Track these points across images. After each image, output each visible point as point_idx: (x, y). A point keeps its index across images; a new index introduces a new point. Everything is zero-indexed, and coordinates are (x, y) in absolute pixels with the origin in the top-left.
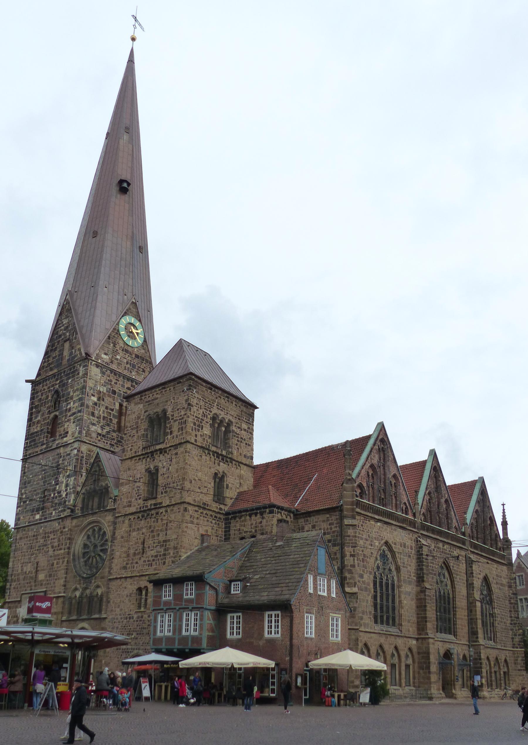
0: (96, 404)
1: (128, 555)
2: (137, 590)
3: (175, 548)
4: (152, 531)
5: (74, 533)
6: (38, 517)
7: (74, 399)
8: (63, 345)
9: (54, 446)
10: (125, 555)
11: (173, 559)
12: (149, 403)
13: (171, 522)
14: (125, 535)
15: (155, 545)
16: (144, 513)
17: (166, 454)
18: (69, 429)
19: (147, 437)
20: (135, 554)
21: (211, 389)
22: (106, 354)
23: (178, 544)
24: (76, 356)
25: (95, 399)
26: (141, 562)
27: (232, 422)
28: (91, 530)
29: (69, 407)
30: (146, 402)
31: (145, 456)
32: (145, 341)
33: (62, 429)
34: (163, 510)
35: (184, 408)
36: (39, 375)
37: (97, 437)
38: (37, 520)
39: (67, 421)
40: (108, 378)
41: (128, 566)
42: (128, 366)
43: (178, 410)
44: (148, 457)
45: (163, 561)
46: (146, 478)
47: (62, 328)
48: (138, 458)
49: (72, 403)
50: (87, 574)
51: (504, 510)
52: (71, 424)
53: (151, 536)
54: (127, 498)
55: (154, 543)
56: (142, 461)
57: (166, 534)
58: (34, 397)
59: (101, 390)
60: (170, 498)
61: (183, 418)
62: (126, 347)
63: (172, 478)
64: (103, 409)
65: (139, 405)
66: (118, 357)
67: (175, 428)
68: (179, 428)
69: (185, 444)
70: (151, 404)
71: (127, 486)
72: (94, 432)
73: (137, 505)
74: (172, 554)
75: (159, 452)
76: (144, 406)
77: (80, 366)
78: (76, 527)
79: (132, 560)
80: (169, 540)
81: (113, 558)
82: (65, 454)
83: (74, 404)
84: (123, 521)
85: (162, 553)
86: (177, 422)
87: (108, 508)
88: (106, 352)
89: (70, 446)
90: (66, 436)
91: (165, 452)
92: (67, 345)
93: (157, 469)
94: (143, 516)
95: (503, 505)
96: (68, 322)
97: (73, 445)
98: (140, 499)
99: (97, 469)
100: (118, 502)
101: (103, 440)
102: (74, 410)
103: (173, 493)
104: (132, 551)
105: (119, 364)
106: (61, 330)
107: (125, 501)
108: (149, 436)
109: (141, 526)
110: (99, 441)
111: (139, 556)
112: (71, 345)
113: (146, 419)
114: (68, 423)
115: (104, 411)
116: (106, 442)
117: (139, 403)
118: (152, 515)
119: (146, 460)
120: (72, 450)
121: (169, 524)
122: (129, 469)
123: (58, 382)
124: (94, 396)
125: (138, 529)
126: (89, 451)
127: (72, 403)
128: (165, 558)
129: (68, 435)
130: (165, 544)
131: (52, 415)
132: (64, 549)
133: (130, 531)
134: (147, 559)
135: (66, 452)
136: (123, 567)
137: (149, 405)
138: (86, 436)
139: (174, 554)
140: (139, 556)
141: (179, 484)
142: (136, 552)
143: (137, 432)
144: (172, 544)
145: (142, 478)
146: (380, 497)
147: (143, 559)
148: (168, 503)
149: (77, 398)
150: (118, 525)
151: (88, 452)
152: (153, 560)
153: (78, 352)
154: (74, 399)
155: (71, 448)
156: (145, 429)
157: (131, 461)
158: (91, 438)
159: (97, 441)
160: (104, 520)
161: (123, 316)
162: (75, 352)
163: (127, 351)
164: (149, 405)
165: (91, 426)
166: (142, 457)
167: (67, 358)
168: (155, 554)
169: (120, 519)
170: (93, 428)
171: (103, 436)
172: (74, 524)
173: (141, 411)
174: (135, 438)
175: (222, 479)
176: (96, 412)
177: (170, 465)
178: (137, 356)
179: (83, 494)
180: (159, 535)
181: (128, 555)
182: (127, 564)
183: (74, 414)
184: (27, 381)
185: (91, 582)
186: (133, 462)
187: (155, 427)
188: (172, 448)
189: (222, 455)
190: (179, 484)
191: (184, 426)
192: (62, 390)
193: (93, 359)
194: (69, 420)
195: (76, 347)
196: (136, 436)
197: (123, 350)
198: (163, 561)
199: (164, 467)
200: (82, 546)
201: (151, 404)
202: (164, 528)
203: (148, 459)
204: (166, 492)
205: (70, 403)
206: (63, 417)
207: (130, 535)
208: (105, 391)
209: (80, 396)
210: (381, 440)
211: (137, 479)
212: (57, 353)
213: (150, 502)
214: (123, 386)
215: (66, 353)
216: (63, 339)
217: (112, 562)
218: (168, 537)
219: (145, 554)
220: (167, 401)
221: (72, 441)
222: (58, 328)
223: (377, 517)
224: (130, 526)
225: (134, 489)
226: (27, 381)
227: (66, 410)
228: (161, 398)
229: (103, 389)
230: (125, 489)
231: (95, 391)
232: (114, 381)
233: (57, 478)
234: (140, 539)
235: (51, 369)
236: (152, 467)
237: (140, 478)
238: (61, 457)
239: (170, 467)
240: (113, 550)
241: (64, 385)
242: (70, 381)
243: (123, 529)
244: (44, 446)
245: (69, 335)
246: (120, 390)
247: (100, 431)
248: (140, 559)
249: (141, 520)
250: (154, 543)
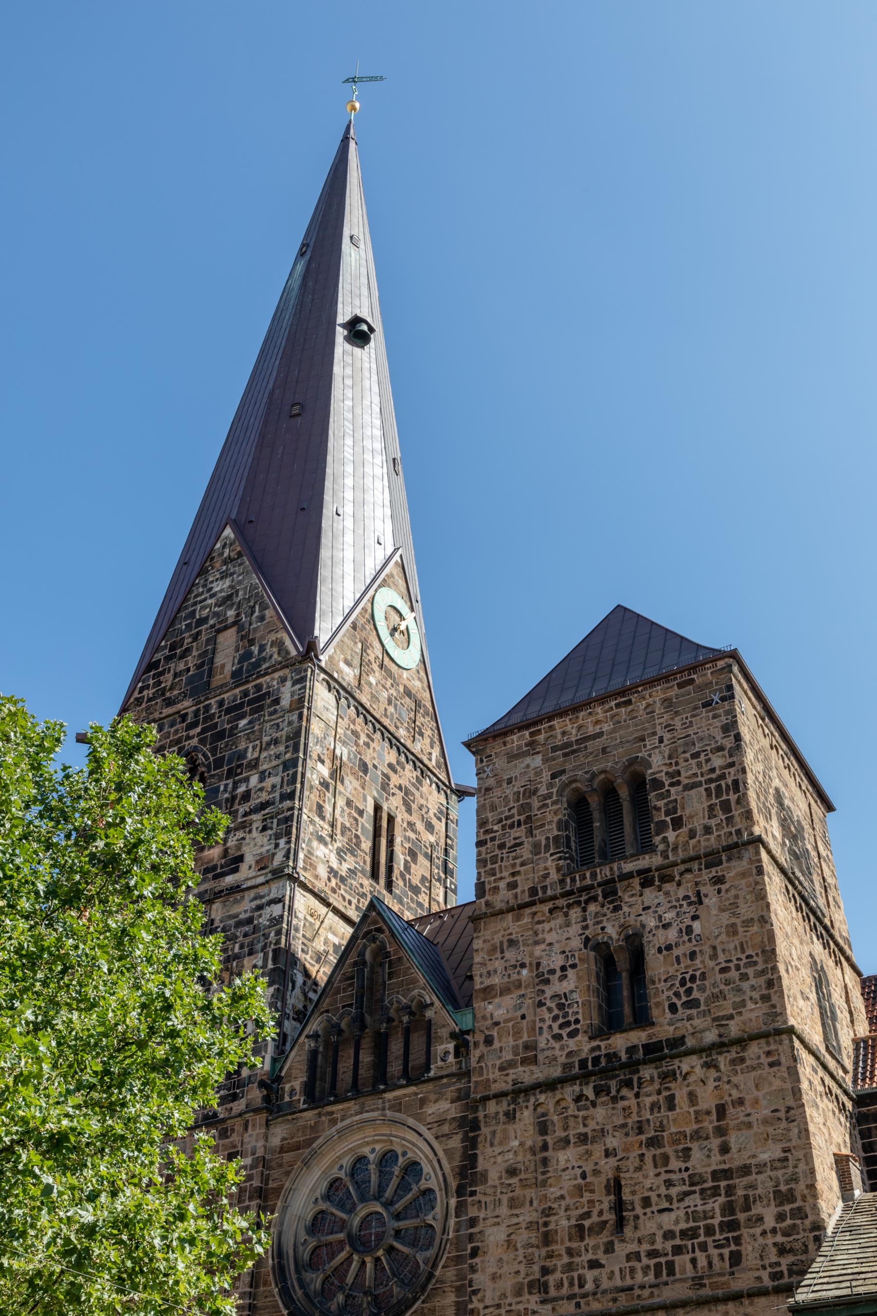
0: (325, 785)
1: (547, 1239)
3: (783, 1197)
4: (654, 1142)
5: (275, 1174)
7: (261, 768)
10: (533, 1237)
11: (779, 1238)
12: (569, 749)
13: (741, 1102)
14: (524, 1159)
15: (674, 1191)
17: (667, 887)
18: (245, 849)
19: (568, 846)
20: (580, 1232)
21: (763, 719)
22: (348, 663)
23: (794, 1179)
25: (324, 771)
26: (615, 1263)
29: (242, 789)
30: (555, 749)
31: (579, 897)
34: (691, 1064)
35: (721, 749)
37: (329, 879)
40: (352, 726)
41: (552, 1279)
43: (696, 755)
44: (594, 899)
45: (726, 1252)
46: (590, 963)
47: (209, 601)
48: (546, 908)
49: (254, 780)
52: (255, 834)
53: (648, 1159)
54: (517, 1034)
55: (669, 1184)
56: (566, 915)
57: (725, 1149)
59: (338, 752)
60: (720, 1021)
61: (722, 777)
63: (714, 956)
64: (341, 802)
65: (528, 760)
66: (373, 680)
67: (696, 805)
68: (711, 808)
69: (751, 848)
70: (573, 752)
71: (509, 1001)
72: (323, 863)
74: (770, 1222)
75: (636, 882)
76: (545, 761)
77: (283, 680)
78: (282, 1150)
79: (570, 1252)
80: (745, 1170)
81: (475, 1253)
82: (232, 922)
83: (262, 780)
84: (511, 1116)
85: (716, 1222)
86: (702, 789)
87: (432, 1074)
88: (349, 658)
89: (252, 893)
90: (236, 870)
96: (231, 587)
97: (262, 890)
98: (572, 1034)
100: (475, 1054)
101: (342, 892)
102: (264, 797)
103: (728, 1004)
104: (562, 1223)
107: (506, 1046)
108: (573, 845)
109: (592, 1125)
110: (334, 891)
111: (604, 1238)
112: (242, 638)
113: (560, 793)
114: (240, 834)
115: (343, 811)
116: (348, 897)
117: (526, 754)
119: (584, 910)
120: (260, 908)
121: (731, 1111)
122: (512, 943)
123: (199, 729)
124: (323, 762)
125: (583, 1139)
126: (312, 915)
127: (254, 780)
128: (737, 1240)
129: (244, 867)
130: (723, 1184)
133: (545, 1147)
134: (646, 1247)
135: (236, 916)
136: (531, 1285)
137: (565, 755)
138: (305, 869)
139: (780, 1217)
140: (604, 1238)
141: (750, 971)
142: (587, 1223)
143: (530, 833)
144: (763, 1183)
145: (574, 966)
147: (622, 1250)
148: (711, 1037)
149: (274, 763)
150: (485, 1130)
151: (309, 917)
152: (678, 1250)
154: (261, 768)
155: (258, 902)
156: (560, 822)
157: (518, 918)
158: (317, 877)
160: (419, 1118)
162: (262, 648)
163: (390, 674)
164: (565, 755)
165: (315, 844)
166: (562, 902)
167: (229, 669)
168: (683, 1226)
169: (492, 1107)
170: (321, 851)
171: (343, 880)
172: (275, 1141)
173: (538, 773)
174: (525, 852)
176: (328, 808)
177: (695, 918)
178: (408, 693)
179: (315, 1036)
180: (686, 1153)
181: (547, 1239)
182: (545, 1271)
183: (263, 806)
186: (526, 920)
188: (695, 866)
190: (750, 971)
191: (733, 797)
192: (214, 751)
193: (323, 664)
195: (263, 637)
196: (526, 845)
198: (726, 1252)
199: (666, 926)
201: (573, 752)
202: (709, 1124)
203: (592, 908)
204: (692, 1004)
205: (247, 780)
207: (545, 1162)
208: (345, 758)
209: (288, 756)
211: (552, 972)
212: (191, 661)
213: (620, 1042)
214: (381, 757)
216: (212, 626)
217: (473, 1269)
218: (736, 1160)
219: (628, 1231)
220: (642, 739)
221: (261, 880)
222: (195, 604)
224: (543, 1128)
225: (541, 1004)
227: (234, 798)
228: (614, 731)
229: (342, 751)
230: (499, 1009)
231: (325, 751)
232: (363, 738)
234: (596, 1172)
235: (169, 703)
236: (612, 931)
237: (563, 968)
239: (697, 926)
240: (473, 1222)
241: (221, 736)
242: (243, 723)
243: (507, 1145)
245: (238, 615)
246: (375, 767)
247: (335, 864)
248: (609, 1248)
249: (594, 1104)
250: (669, 1184)
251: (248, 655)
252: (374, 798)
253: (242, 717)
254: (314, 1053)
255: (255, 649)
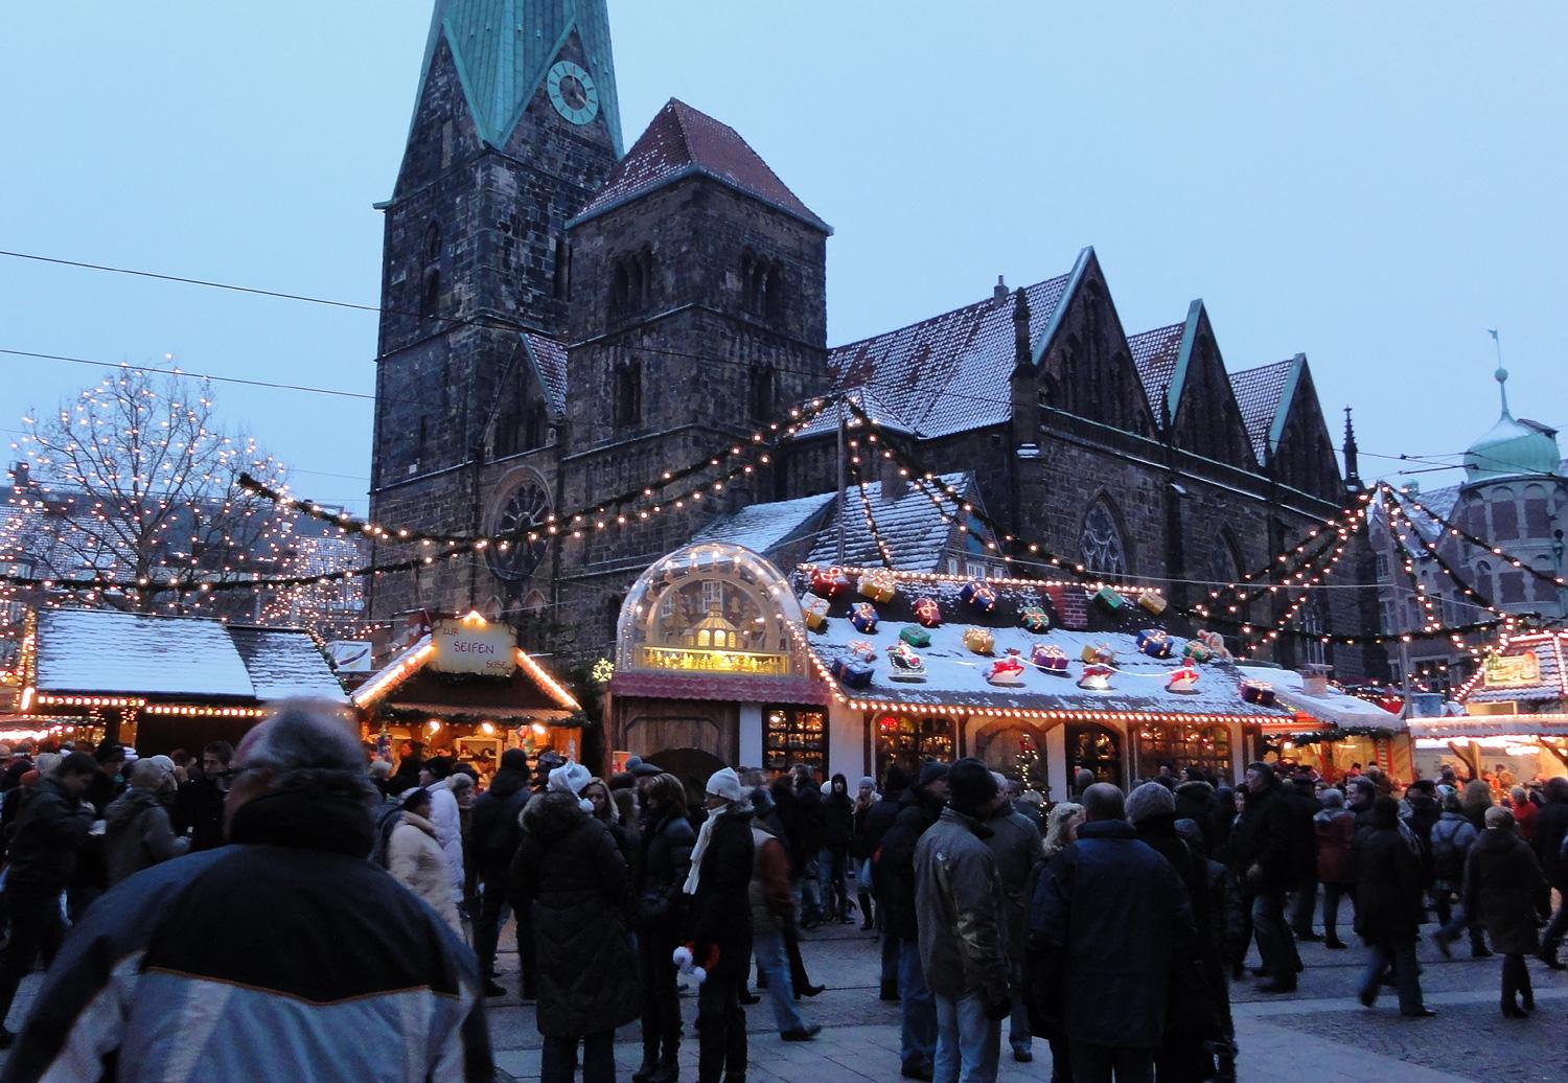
2: (610, 601)
6: (413, 469)
8: (441, 128)
9: (436, 331)
16: (616, 455)
24: (466, 150)
27: (781, 264)
28: (516, 491)
32: (600, 112)
33: (448, 296)
36: (398, 192)
37: (518, 309)
38: (412, 475)
39: (457, 281)
42: (571, 163)
47: (437, 95)
50: (513, 574)
51: (1349, 421)
58: (391, 237)
62: (564, 126)
73: (603, 438)
77: (476, 168)
91: (653, 330)
92: (448, 129)
93: (636, 365)
94: (614, 459)
95: (1348, 410)
96: (448, 83)
99: (522, 370)
105: (552, 161)
106: (434, 99)
114: (460, 285)
118: (632, 455)
131: (428, 270)
132: (467, 529)
143: (595, 294)
146: (1090, 401)
153: (470, 142)
159: (516, 316)
161: (554, 63)
171: (529, 306)
175: (766, 379)
179: (497, 420)
184: (377, 206)
185: (521, 591)
187: (630, 280)
189: (764, 330)
194: (460, 280)
197: (557, 133)
200: (500, 519)
206: (449, 272)
210: (1091, 291)
215: (447, 147)
223: (1084, 442)
226: (377, 206)
233: (445, 392)
236: (627, 361)
238: (450, 350)
242: (458, 200)
244: (417, 332)
251: (457, 145)
252: (556, 238)
253: (457, 196)
254: (498, 429)
255: (461, 139)
